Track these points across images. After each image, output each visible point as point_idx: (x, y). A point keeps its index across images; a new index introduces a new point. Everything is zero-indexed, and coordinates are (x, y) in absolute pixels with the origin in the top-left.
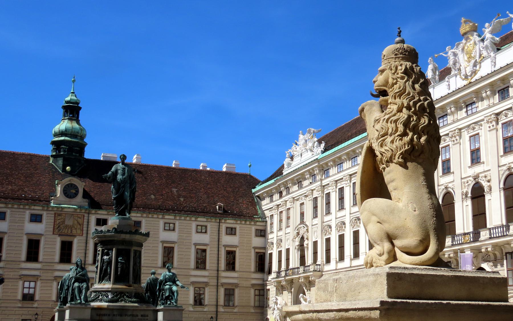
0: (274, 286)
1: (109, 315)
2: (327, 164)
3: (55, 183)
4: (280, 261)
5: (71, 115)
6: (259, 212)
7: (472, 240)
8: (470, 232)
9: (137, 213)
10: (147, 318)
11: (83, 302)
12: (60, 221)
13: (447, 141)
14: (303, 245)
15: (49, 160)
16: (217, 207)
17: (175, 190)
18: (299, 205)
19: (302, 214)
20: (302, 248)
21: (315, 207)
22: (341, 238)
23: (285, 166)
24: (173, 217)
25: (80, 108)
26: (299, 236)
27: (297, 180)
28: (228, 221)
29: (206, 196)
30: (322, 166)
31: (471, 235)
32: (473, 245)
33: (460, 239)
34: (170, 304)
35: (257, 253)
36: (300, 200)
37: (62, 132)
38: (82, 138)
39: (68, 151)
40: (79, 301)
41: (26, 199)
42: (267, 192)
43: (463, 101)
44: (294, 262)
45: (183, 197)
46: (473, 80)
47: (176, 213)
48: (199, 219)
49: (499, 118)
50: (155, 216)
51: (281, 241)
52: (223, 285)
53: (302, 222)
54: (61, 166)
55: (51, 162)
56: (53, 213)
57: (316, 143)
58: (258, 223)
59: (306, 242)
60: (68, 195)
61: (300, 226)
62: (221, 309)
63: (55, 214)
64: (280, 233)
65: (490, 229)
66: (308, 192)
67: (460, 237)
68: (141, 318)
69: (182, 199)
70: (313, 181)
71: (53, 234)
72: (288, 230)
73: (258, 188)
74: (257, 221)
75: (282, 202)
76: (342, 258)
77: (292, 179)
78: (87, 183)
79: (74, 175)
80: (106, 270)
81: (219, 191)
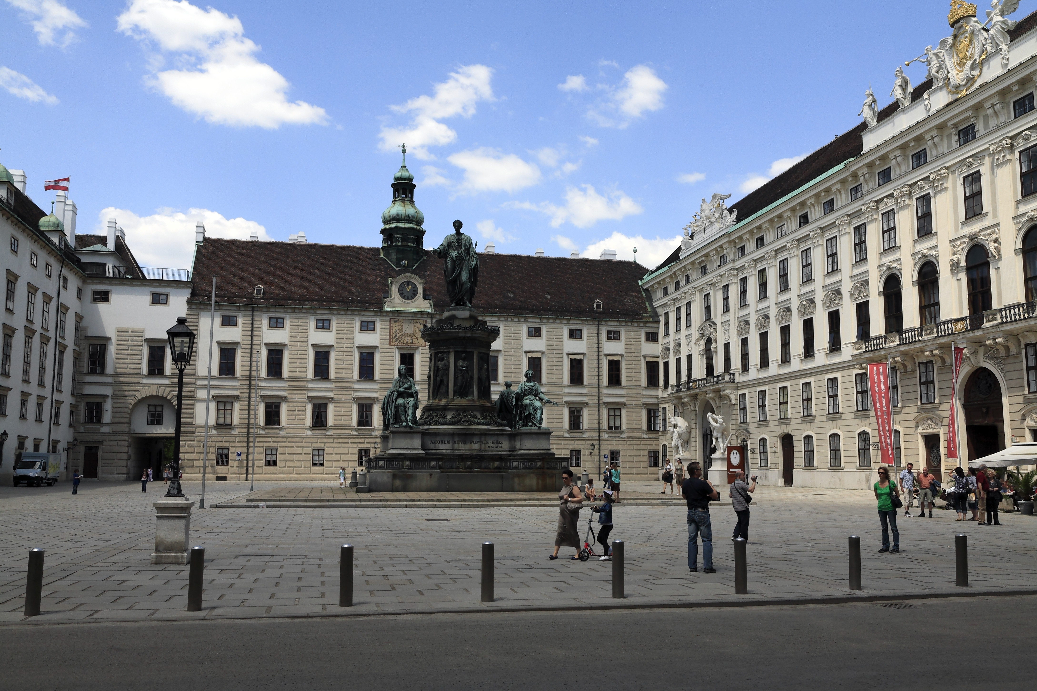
0: (673, 404)
1: (448, 442)
2: (740, 238)
3: (388, 282)
4: (679, 372)
5: (404, 196)
6: (649, 309)
7: (969, 328)
8: (966, 317)
9: (493, 316)
10: (500, 445)
11: (410, 424)
12: (396, 328)
13: (925, 188)
15: (379, 255)
16: (595, 305)
17: (539, 285)
19: (708, 308)
20: (709, 354)
21: (726, 299)
22: (764, 337)
23: (683, 247)
24: (538, 320)
25: (414, 186)
27: (700, 263)
28: (610, 323)
30: (734, 241)
31: (968, 321)
32: (971, 334)
33: (950, 327)
34: (531, 426)
35: (648, 362)
36: (704, 290)
37: (393, 216)
38: (420, 222)
39: (402, 241)
40: (404, 424)
41: (352, 301)
42: (659, 283)
43: (952, 125)
44: (699, 372)
45: (549, 294)
46: (968, 92)
47: (542, 315)
48: (571, 322)
49: (1015, 144)
50: (516, 320)
51: (680, 345)
52: (606, 404)
53: (708, 317)
54: (395, 260)
55: (382, 256)
56: (388, 318)
57: (726, 211)
58: (648, 325)
59: (713, 345)
60: (405, 296)
62: (605, 435)
63: (390, 319)
65: (1000, 310)
66: (715, 279)
67: (950, 325)
68: (492, 445)
69: (549, 297)
70: (722, 263)
71: (390, 344)
73: (646, 278)
74: (647, 322)
75: (679, 294)
76: (764, 363)
77: (693, 263)
78: (428, 280)
79: (413, 272)
80: (442, 381)
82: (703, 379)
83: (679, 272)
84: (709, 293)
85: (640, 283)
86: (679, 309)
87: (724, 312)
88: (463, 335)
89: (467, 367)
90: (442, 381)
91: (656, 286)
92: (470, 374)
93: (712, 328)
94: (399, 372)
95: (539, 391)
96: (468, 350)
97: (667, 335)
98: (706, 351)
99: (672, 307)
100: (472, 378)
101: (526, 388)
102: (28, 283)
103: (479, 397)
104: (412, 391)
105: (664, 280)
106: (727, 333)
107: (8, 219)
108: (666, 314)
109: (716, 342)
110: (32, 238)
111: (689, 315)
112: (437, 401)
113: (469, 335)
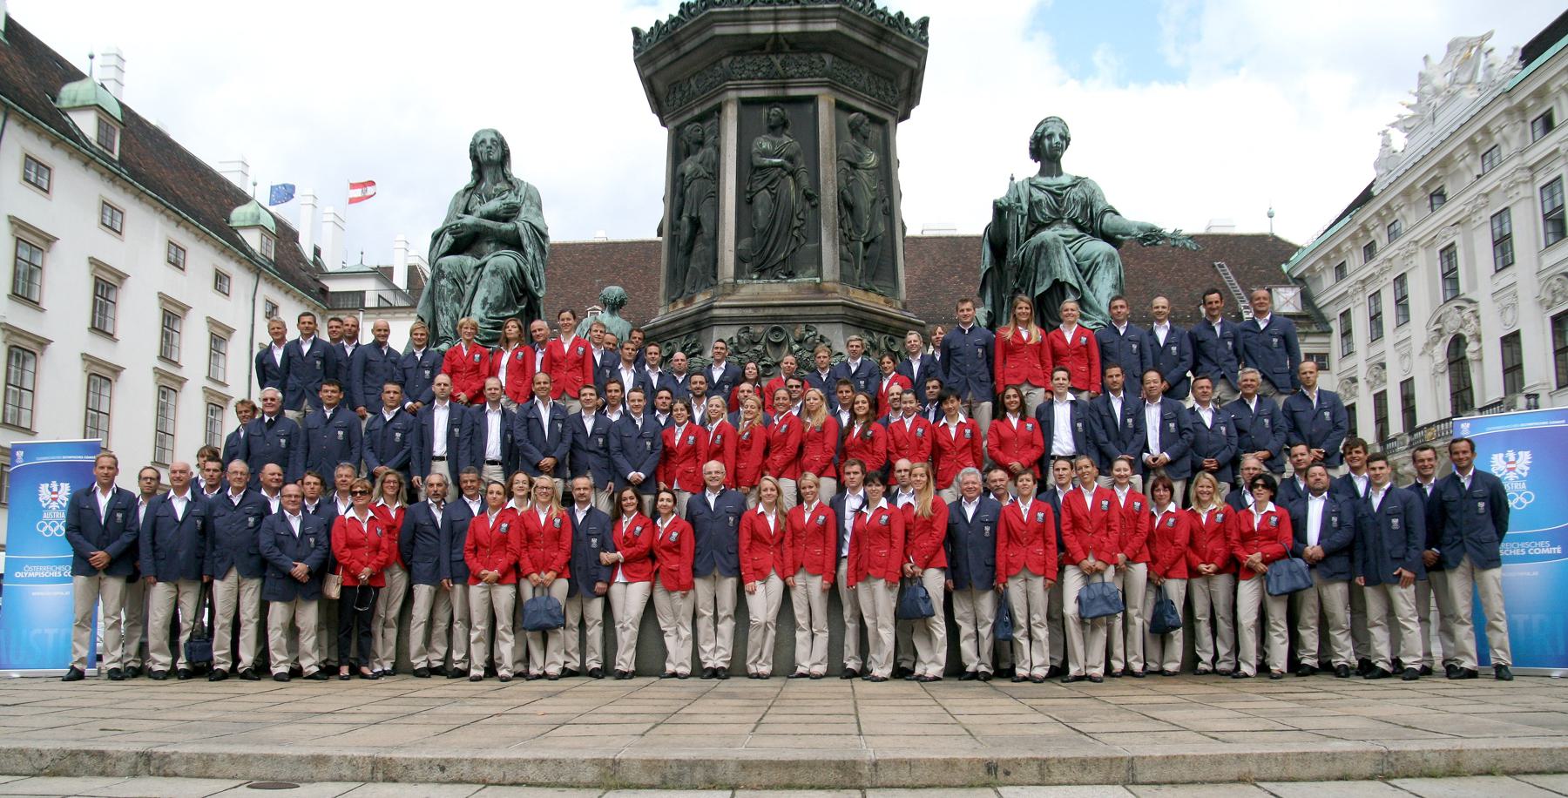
14: (1465, 357)
18: (1438, 255)
19: (1450, 277)
26: (1442, 339)
29: (1170, 287)
42: (1326, 258)
51: (1383, 366)
59: (1471, 348)
61: (1447, 309)
64: (1375, 350)
72: (1404, 333)
73: (1295, 258)
77: (1407, 193)
80: (696, 224)
81: (1203, 275)
82: (1448, 420)
83: (1375, 221)
84: (1453, 244)
85: (1284, 267)
86: (1376, 295)
87: (1497, 271)
88: (770, 29)
89: (790, 159)
90: (696, 224)
91: (1321, 265)
92: (805, 182)
93: (1466, 314)
94: (475, 157)
95: (1099, 207)
96: (793, 92)
97: (1348, 353)
98: (1450, 364)
99: (1360, 296)
100: (811, 197)
101: (1038, 195)
102: (159, 293)
103: (844, 279)
104: (521, 224)
105: (1337, 250)
106: (1509, 315)
107: (86, 164)
108: (1346, 315)
109: (1479, 340)
110: (168, 216)
111: (1402, 303)
112: (680, 305)
113: (792, 28)
